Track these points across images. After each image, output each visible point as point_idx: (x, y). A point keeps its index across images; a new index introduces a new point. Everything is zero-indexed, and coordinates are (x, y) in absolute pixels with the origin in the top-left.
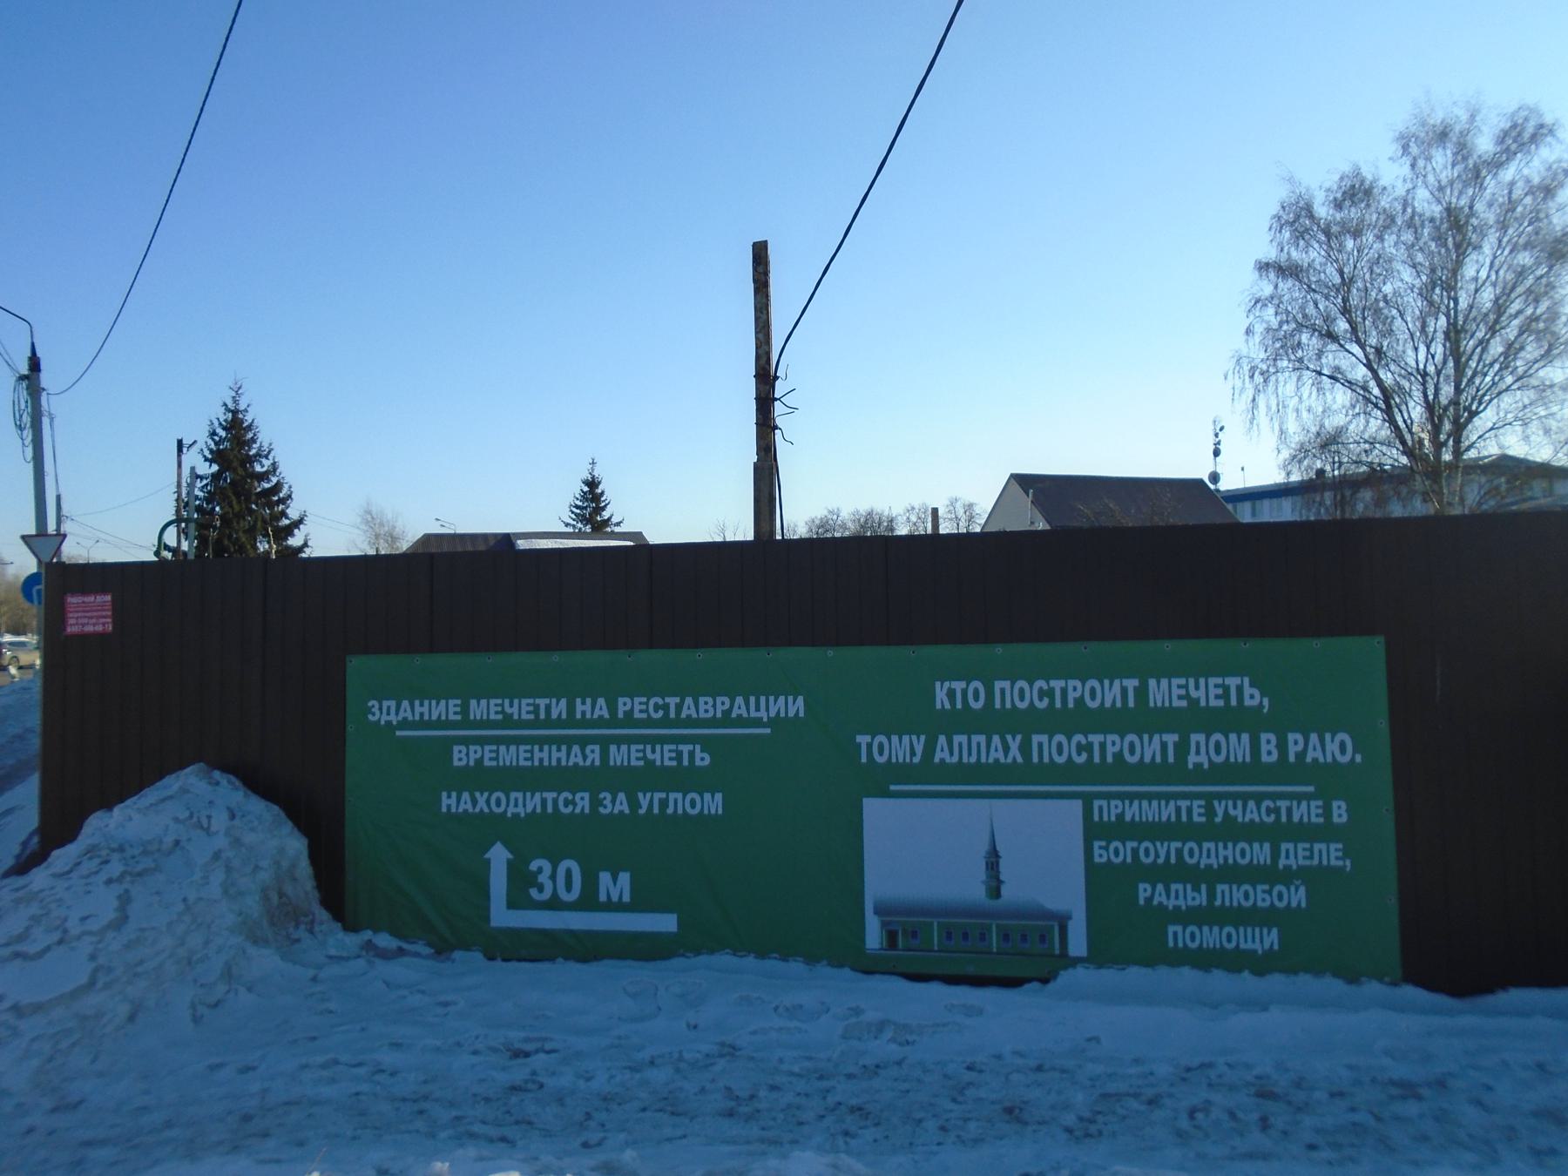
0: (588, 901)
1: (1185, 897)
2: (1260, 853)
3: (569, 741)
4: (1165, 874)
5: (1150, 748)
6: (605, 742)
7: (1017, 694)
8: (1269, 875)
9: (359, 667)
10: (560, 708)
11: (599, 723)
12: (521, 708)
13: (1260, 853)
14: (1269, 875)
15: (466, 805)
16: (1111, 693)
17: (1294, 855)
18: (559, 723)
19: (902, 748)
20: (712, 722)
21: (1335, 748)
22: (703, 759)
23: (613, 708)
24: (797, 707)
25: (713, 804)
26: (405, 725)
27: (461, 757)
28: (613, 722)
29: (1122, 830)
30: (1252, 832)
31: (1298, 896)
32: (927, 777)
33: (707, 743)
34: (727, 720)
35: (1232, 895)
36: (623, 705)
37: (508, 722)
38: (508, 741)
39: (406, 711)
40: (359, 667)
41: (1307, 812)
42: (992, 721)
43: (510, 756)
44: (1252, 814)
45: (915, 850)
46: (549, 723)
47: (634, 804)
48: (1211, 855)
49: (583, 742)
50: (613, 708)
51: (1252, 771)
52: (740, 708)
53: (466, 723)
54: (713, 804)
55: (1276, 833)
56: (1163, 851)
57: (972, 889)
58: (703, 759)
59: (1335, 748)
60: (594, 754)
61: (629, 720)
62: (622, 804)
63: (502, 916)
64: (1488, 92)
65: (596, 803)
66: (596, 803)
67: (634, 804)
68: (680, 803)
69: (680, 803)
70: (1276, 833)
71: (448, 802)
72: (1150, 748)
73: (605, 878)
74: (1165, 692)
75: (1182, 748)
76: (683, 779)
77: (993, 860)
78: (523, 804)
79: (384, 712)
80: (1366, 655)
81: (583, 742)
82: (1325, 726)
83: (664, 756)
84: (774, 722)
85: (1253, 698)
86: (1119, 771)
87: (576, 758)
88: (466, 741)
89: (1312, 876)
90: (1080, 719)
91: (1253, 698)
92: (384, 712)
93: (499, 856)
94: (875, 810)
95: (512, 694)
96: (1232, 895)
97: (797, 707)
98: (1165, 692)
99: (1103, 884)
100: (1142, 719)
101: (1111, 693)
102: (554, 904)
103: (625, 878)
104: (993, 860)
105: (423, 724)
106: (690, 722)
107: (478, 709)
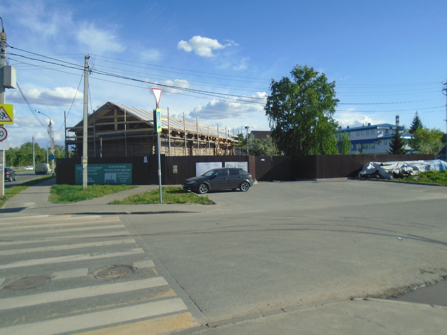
1: (121, 179)
4: (121, 177)
5: (120, 170)
7: (113, 167)
8: (126, 177)
9: (76, 165)
14: (126, 177)
16: (118, 167)
17: (127, 176)
19: (107, 170)
21: (129, 170)
24: (101, 168)
25: (96, 174)
29: (119, 175)
35: (124, 179)
40: (76, 165)
42: (112, 168)
45: (108, 176)
48: (123, 176)
51: (125, 171)
54: (96, 174)
55: (126, 175)
59: (129, 170)
64: (304, 62)
70: (126, 175)
72: (120, 170)
74: (121, 167)
76: (95, 172)
80: (130, 165)
82: (128, 169)
89: (128, 177)
90: (116, 168)
94: (106, 174)
96: (124, 179)
97: (101, 168)
98: (121, 167)
99: (117, 178)
100: (120, 168)
101: (118, 167)
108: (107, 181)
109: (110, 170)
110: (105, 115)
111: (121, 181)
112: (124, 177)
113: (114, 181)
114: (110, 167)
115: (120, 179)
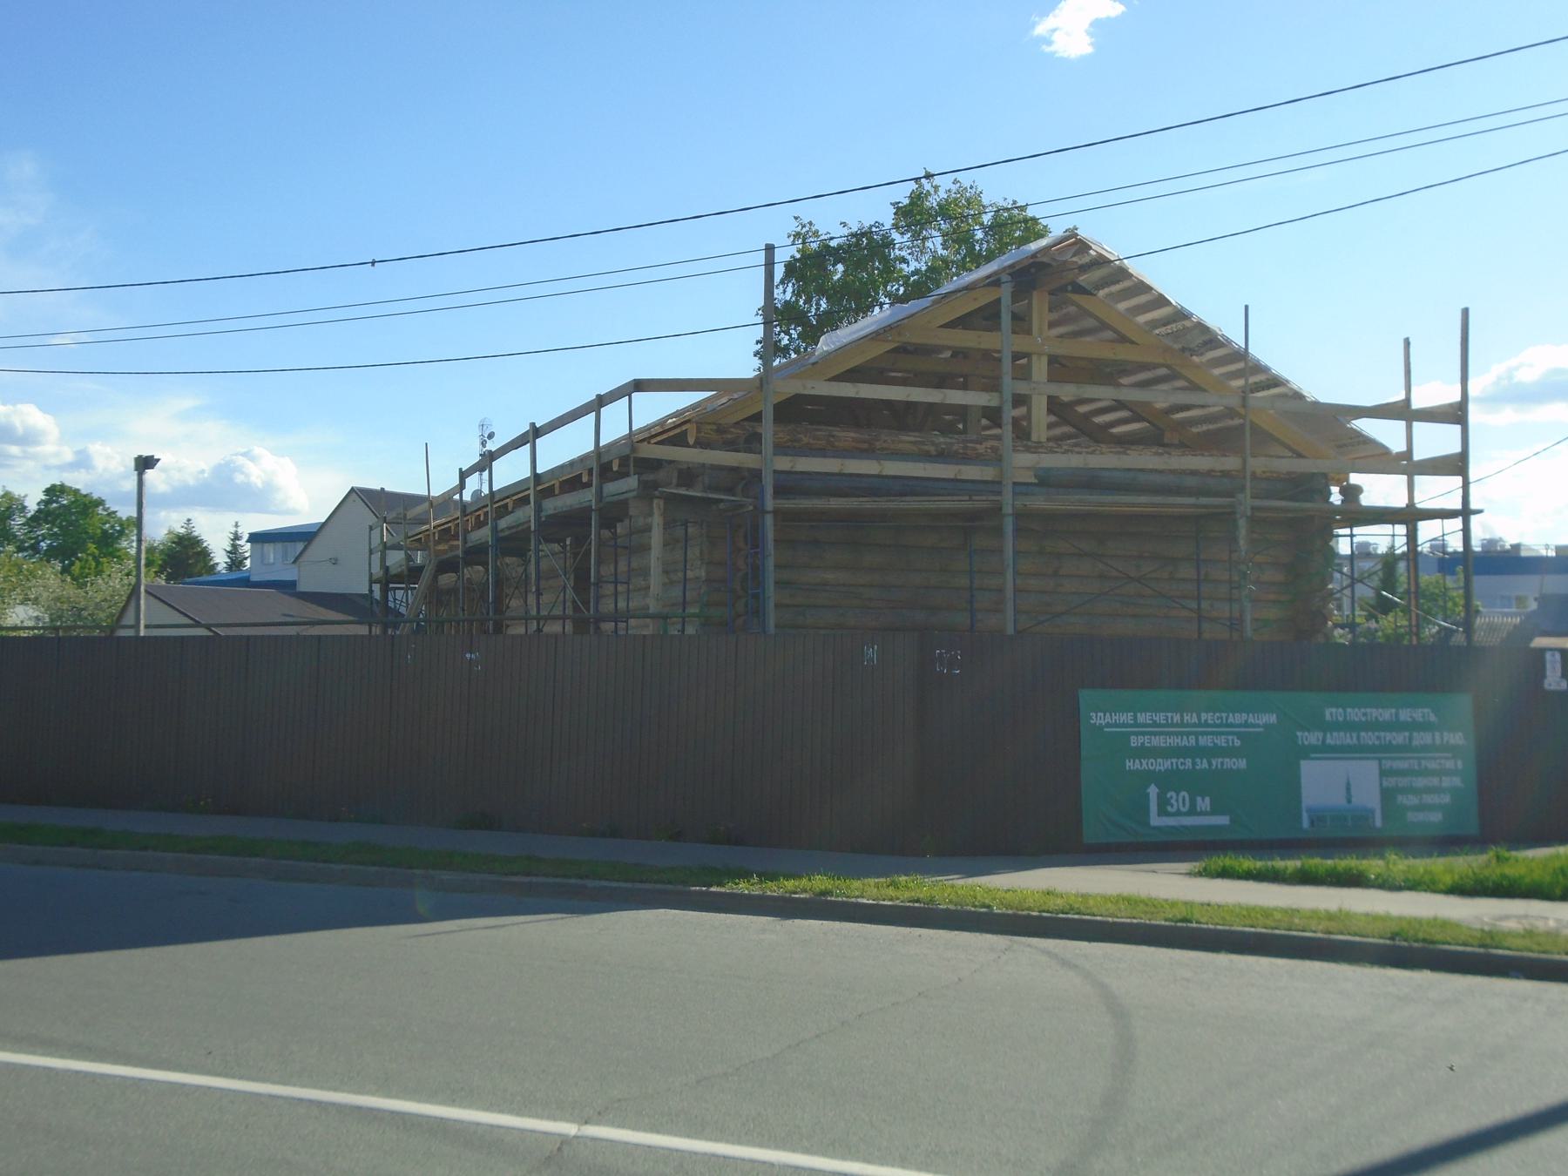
0: (1193, 812)
1: (1412, 800)
2: (1435, 781)
3: (1182, 734)
5: (1399, 738)
6: (1196, 734)
7: (1355, 714)
8: (1437, 790)
9: (1086, 696)
10: (1177, 718)
11: (1194, 725)
12: (1160, 717)
13: (1435, 781)
14: (1437, 790)
15: (1138, 766)
16: (1386, 714)
17: (1447, 782)
18: (1177, 725)
20: (1240, 726)
21: (1457, 739)
22: (1238, 743)
23: (1199, 718)
24: (1273, 719)
25: (1242, 764)
26: (1108, 725)
27: (1135, 742)
28: (1199, 725)
30: (1433, 773)
31: (1447, 799)
32: (1325, 751)
33: (1240, 736)
34: (1246, 725)
36: (1204, 716)
37: (1155, 724)
38: (1155, 734)
39: (1108, 719)
40: (1086, 696)
41: (1449, 764)
43: (1157, 741)
44: (1432, 765)
45: (1327, 784)
46: (1172, 725)
47: (1210, 764)
48: (1420, 782)
49: (1188, 734)
50: (1199, 718)
52: (1251, 720)
53: (1136, 725)
54: (1242, 764)
56: (1403, 782)
57: (1343, 802)
58: (1238, 743)
59: (1457, 739)
60: (1192, 740)
61: (1206, 725)
62: (1205, 765)
63: (1155, 821)
65: (1194, 764)
66: (1194, 764)
67: (1210, 764)
68: (1230, 763)
69: (1230, 763)
71: (1129, 764)
72: (1399, 738)
73: (1199, 799)
74: (1405, 715)
75: (1411, 739)
76: (1229, 752)
77: (1348, 789)
78: (1162, 765)
79: (1098, 719)
81: (1188, 734)
83: (1221, 741)
84: (1266, 726)
85: (1433, 718)
86: (1389, 748)
87: (1185, 742)
88: (1136, 734)
91: (1433, 718)
92: (1098, 719)
93: (1153, 791)
95: (1157, 710)
96: (1429, 799)
97: (1273, 719)
98: (1405, 715)
99: (1387, 795)
101: (1386, 714)
102: (1178, 813)
103: (1207, 799)
104: (1348, 789)
105: (1116, 725)
106: (1231, 725)
107: (1141, 718)
108: (1317, 818)
109: (1333, 739)
110: (951, 325)
111: (1412, 817)
112: (1429, 790)
113: (1364, 816)
114: (1330, 713)
115: (1401, 799)
